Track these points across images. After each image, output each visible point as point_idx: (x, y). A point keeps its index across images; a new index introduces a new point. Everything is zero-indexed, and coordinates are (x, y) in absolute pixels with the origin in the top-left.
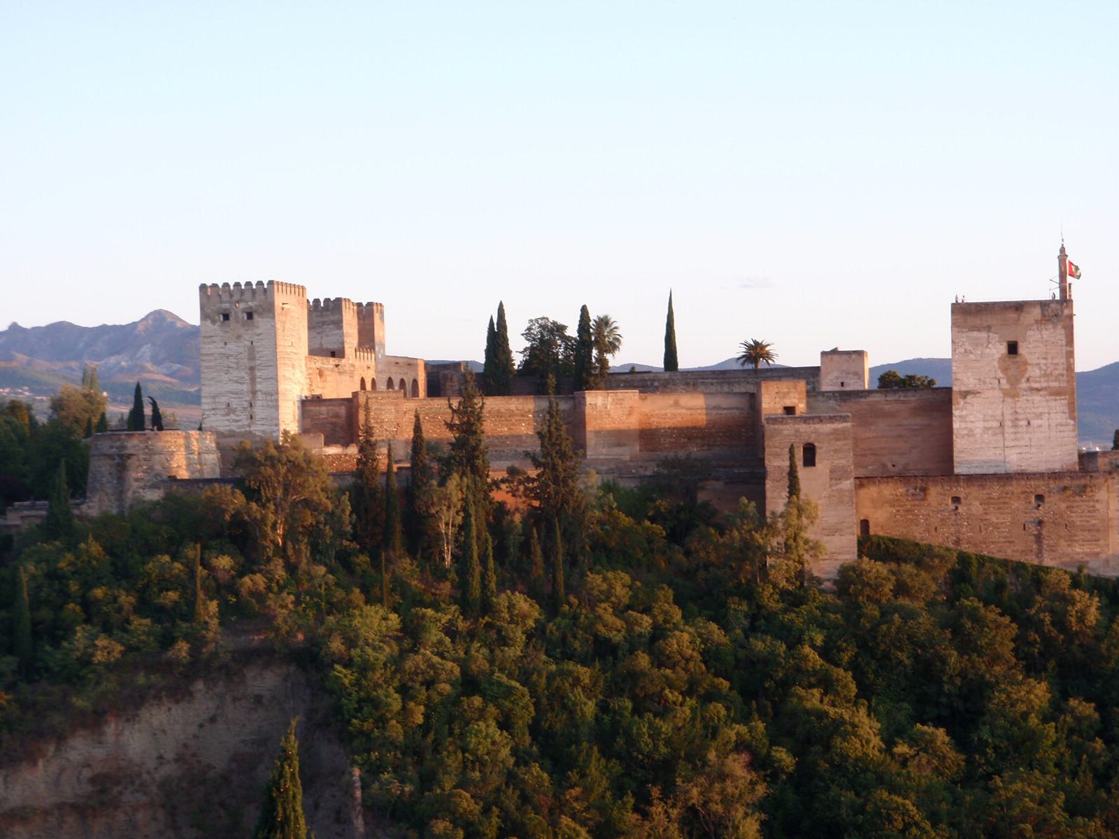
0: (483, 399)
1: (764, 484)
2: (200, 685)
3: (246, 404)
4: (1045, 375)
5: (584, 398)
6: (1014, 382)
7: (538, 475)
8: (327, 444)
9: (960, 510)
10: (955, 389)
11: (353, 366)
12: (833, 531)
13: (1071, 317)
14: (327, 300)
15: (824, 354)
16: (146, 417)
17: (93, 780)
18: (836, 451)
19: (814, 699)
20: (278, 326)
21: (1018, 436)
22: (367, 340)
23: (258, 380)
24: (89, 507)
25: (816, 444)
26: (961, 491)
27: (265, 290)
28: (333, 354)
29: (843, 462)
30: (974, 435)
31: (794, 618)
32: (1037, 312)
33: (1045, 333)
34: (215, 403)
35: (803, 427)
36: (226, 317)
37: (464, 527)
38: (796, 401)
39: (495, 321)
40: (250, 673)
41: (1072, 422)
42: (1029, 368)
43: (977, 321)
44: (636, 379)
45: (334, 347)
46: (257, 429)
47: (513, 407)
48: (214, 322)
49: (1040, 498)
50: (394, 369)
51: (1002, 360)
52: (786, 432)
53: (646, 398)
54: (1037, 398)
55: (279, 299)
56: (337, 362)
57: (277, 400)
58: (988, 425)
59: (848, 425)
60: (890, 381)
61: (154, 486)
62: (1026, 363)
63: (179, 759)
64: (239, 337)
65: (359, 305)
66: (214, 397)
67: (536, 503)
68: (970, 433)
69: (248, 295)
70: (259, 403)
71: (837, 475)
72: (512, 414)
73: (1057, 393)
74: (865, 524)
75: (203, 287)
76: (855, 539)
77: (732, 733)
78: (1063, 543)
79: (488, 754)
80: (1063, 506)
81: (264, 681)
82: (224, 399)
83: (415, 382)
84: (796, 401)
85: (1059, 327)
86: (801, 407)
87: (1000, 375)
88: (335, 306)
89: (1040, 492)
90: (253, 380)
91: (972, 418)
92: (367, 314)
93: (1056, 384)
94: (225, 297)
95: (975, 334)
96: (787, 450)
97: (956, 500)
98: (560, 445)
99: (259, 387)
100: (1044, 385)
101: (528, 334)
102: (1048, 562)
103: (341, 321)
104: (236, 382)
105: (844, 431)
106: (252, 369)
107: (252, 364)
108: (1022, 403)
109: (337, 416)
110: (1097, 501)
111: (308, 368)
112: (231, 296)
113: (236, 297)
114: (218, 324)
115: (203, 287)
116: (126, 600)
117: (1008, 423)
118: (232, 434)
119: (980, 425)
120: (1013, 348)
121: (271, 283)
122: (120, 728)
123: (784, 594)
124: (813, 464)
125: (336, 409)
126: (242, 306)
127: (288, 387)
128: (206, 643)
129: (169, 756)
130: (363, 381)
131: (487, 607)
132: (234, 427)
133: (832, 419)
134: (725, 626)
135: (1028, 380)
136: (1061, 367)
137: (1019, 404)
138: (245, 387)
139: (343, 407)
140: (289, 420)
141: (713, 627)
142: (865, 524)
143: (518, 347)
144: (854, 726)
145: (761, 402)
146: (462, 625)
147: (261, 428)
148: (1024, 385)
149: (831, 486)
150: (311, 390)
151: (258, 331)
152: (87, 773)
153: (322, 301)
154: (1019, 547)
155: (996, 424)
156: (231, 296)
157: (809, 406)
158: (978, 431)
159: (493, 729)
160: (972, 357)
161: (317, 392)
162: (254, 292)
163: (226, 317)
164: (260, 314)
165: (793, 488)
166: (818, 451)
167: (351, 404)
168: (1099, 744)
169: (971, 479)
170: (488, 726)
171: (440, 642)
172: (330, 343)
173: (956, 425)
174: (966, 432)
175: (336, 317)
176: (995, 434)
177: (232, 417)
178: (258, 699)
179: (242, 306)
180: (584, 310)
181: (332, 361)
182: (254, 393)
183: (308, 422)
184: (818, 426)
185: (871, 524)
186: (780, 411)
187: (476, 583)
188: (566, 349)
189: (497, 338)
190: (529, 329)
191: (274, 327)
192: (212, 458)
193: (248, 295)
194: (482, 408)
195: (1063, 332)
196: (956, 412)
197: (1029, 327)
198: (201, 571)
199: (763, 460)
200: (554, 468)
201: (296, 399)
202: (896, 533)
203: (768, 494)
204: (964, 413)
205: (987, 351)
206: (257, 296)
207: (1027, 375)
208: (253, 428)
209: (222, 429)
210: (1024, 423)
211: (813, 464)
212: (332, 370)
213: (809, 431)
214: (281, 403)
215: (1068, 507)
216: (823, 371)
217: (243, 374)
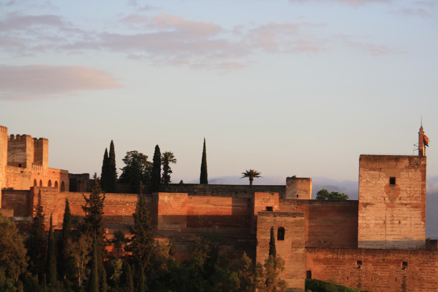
0: (104, 195)
4: (409, 197)
5: (158, 196)
6: (392, 199)
7: (133, 238)
9: (361, 268)
10: (360, 201)
11: (30, 172)
12: (292, 276)
13: (425, 166)
14: (18, 136)
15: (288, 179)
16: (157, 193)
18: (295, 232)
21: (394, 229)
25: (285, 228)
26: (362, 257)
28: (20, 166)
30: (369, 227)
33: (410, 173)
35: (278, 218)
37: (90, 265)
38: (273, 204)
39: (108, 152)
41: (423, 223)
42: (401, 192)
43: (374, 165)
47: (118, 199)
49: (405, 264)
50: (52, 175)
51: (386, 187)
52: (269, 221)
53: (191, 198)
54: (405, 209)
56: (22, 170)
58: (377, 222)
59: (303, 218)
62: (399, 190)
65: (35, 139)
67: (130, 253)
68: (368, 226)
71: (295, 245)
72: (117, 203)
73: (416, 207)
74: (309, 273)
76: (304, 281)
80: (418, 269)
85: (418, 171)
86: (276, 208)
87: (385, 195)
88: (22, 139)
89: (405, 260)
91: (369, 218)
95: (372, 172)
96: (269, 230)
97: (360, 262)
98: (145, 222)
100: (409, 202)
101: (126, 160)
105: (301, 221)
108: (396, 211)
109: (21, 200)
110: (436, 267)
117: (388, 222)
119: (373, 222)
120: (393, 181)
130: (35, 181)
133: (294, 215)
135: (400, 199)
136: (418, 192)
137: (395, 212)
139: (25, 195)
142: (309, 273)
145: (254, 204)
148: (398, 201)
149: (292, 252)
150: (7, 185)
153: (15, 135)
155: (382, 222)
157: (280, 207)
158: (372, 225)
160: (370, 184)
161: (11, 186)
165: (272, 251)
166: (286, 232)
167: (29, 193)
169: (368, 251)
172: (18, 159)
173: (360, 222)
174: (365, 225)
175: (22, 145)
176: (381, 228)
180: (157, 148)
181: (19, 169)
183: (5, 202)
184: (286, 218)
185: (312, 273)
186: (264, 209)
188: (146, 169)
190: (126, 157)
194: (103, 199)
195: (420, 173)
196: (360, 215)
197: (402, 170)
199: (255, 235)
200: (141, 234)
202: (325, 279)
203: (258, 254)
204: (365, 215)
205: (379, 182)
207: (400, 196)
210: (397, 222)
212: (19, 174)
213: (281, 221)
215: (420, 269)
216: (287, 187)
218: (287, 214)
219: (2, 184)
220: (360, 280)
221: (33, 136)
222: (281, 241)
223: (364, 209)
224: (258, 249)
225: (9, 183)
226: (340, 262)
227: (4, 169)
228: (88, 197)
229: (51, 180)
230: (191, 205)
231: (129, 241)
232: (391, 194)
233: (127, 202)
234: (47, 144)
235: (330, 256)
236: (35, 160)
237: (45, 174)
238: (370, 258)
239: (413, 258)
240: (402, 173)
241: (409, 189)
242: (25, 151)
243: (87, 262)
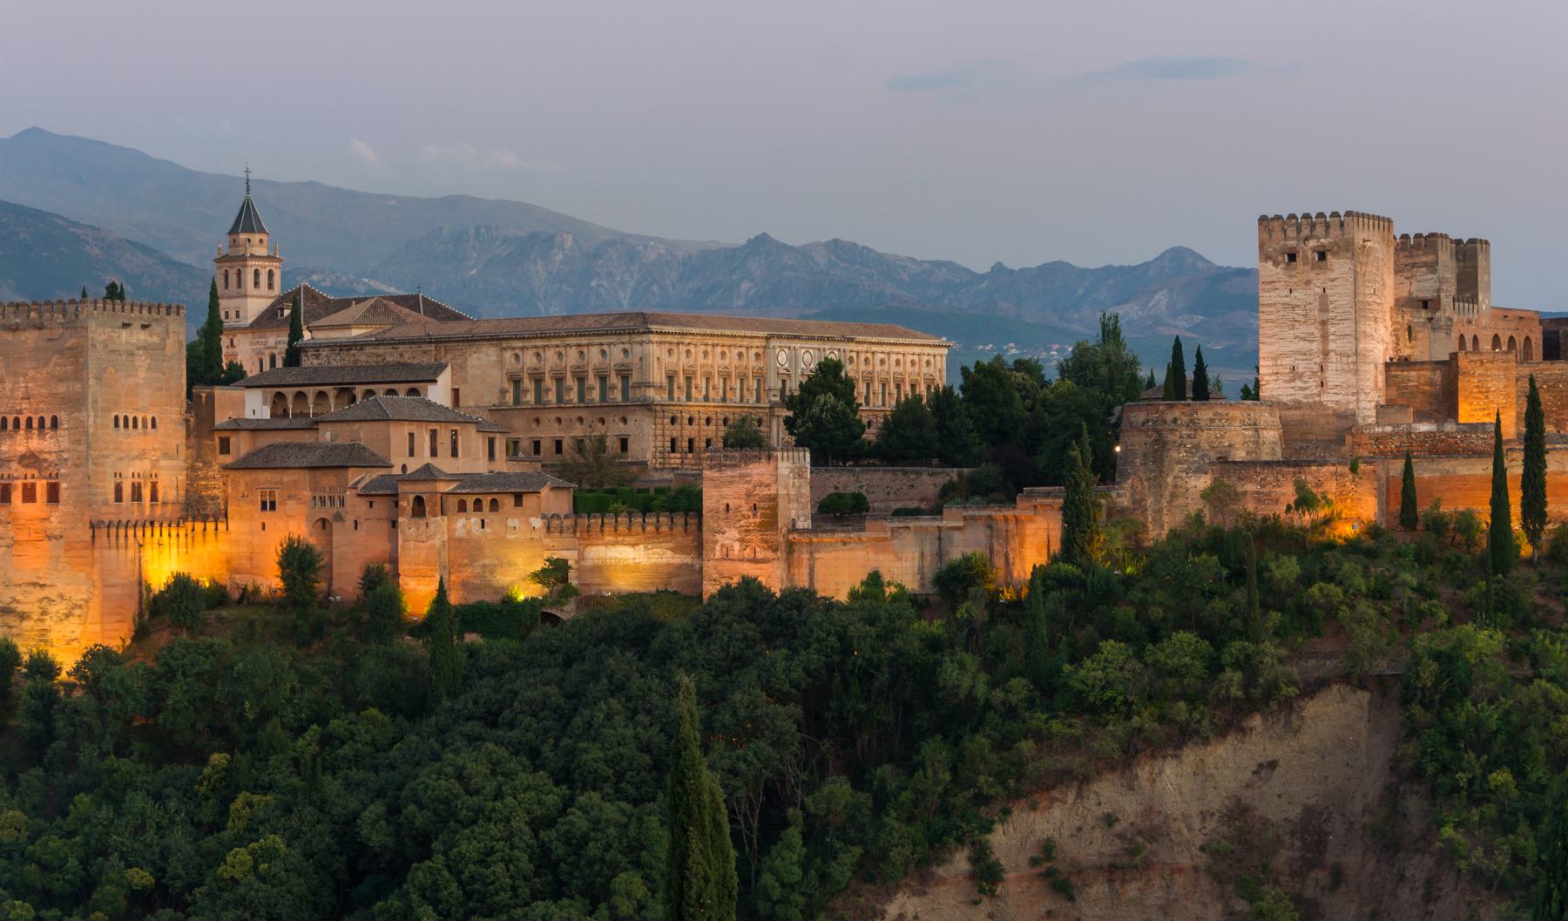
2: (1256, 721)
3: (1316, 368)
8: (1420, 416)
11: (1450, 319)
14: (1418, 236)
22: (1468, 286)
23: (1332, 337)
34: (1276, 365)
36: (1292, 258)
46: (1329, 399)
48: (1276, 264)
50: (1502, 324)
55: (1359, 236)
56: (1430, 315)
61: (1200, 471)
64: (1308, 283)
65: (1459, 242)
66: (1275, 359)
69: (1320, 230)
70: (1332, 366)
75: (1263, 220)
82: (1288, 362)
83: (1527, 339)
88: (1429, 242)
90: (1325, 337)
92: (1469, 255)
94: (1292, 232)
99: (1332, 346)
103: (1437, 263)
104: (1304, 339)
106: (1324, 323)
107: (1324, 316)
111: (1394, 323)
112: (1299, 231)
113: (1306, 232)
114: (1282, 266)
115: (1263, 220)
118: (1298, 405)
121: (1348, 214)
122: (1156, 771)
126: (1312, 243)
127: (1369, 346)
130: (1462, 337)
132: (1299, 396)
138: (1315, 346)
139: (1438, 372)
150: (1397, 350)
151: (1332, 276)
153: (1412, 236)
156: (1299, 231)
161: (1406, 352)
163: (1292, 257)
164: (1335, 254)
175: (1430, 258)
177: (1298, 383)
179: (1312, 243)
181: (1424, 314)
182: (1326, 353)
183: (1393, 393)
192: (1271, 435)
193: (1320, 230)
201: (1381, 361)
206: (1331, 231)
208: (1324, 398)
209: (1285, 399)
212: (1424, 325)
214: (1362, 367)
219: (1387, 349)
221: (1454, 236)
227: (1388, 315)
234: (1487, 252)
236: (1459, 291)
237: (1484, 321)
242: (1434, 271)
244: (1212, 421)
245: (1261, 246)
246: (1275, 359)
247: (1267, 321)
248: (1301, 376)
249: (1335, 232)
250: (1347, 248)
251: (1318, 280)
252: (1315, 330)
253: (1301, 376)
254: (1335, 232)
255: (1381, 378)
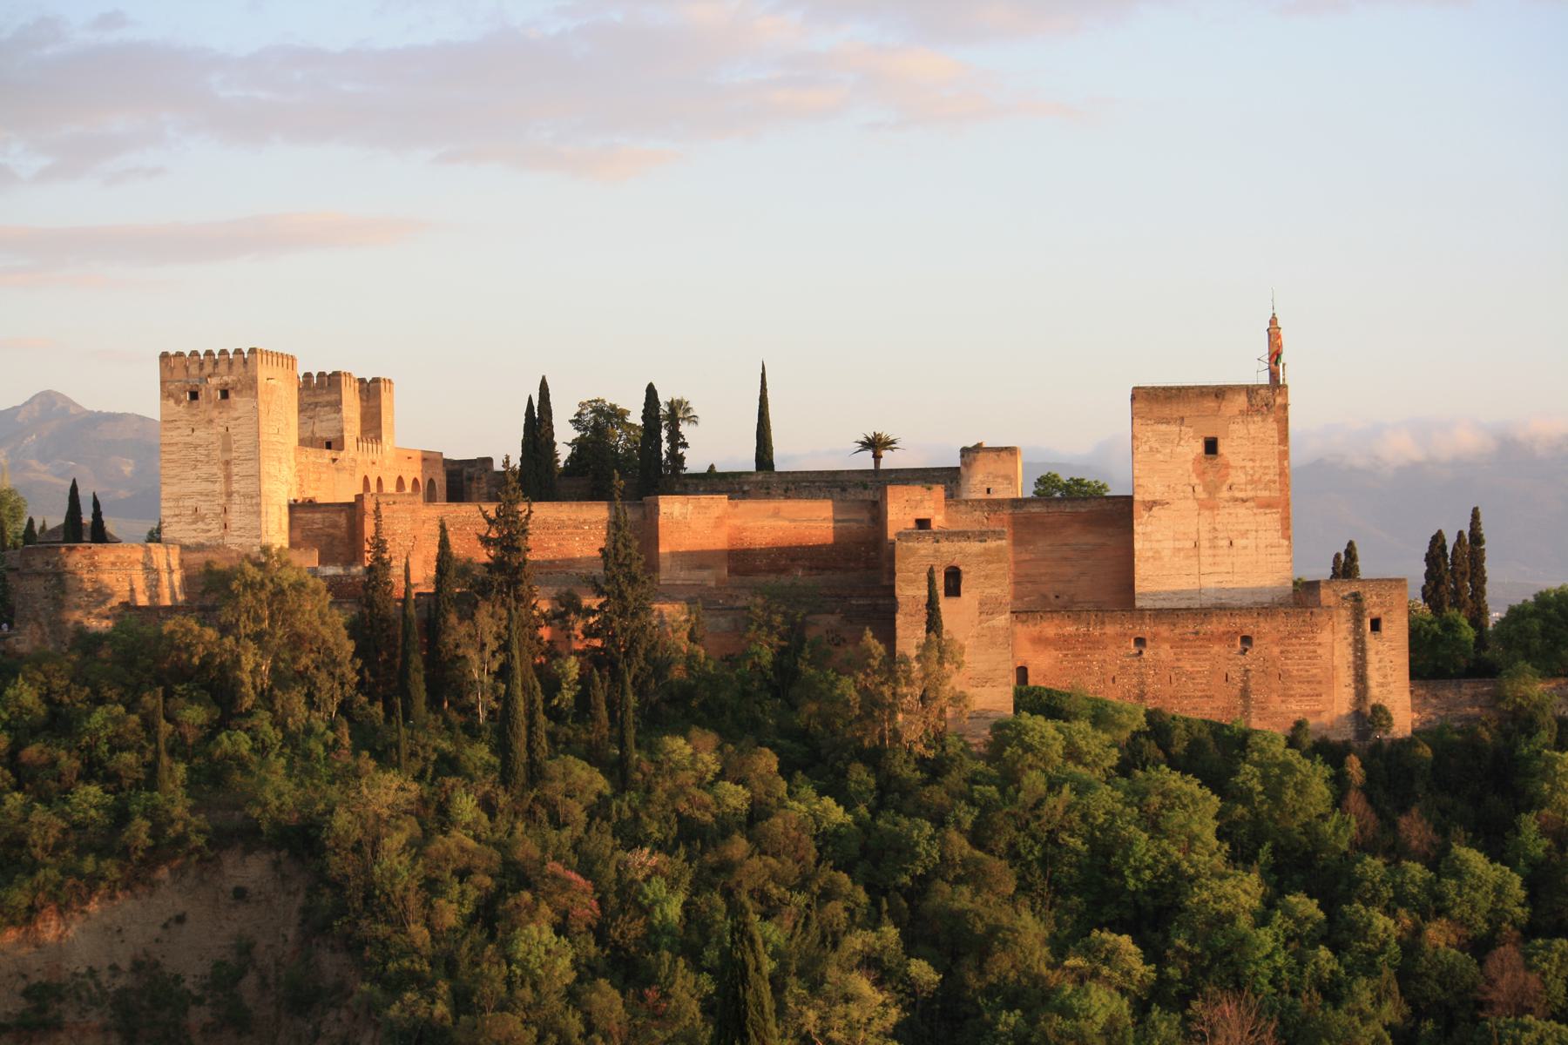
0: (529, 506)
1: (893, 620)
2: (163, 873)
3: (219, 510)
4: (1252, 482)
5: (657, 505)
6: (1212, 490)
7: (601, 606)
9: (1145, 655)
10: (1137, 498)
11: (354, 460)
12: (984, 681)
13: (1285, 407)
14: (321, 375)
16: (654, 497)
17: (26, 993)
18: (986, 577)
19: (963, 898)
20: (262, 408)
21: (1218, 559)
22: (372, 425)
23: (235, 478)
24: (18, 642)
25: (961, 568)
26: (1146, 630)
27: (245, 362)
28: (329, 446)
29: (996, 591)
30: (1161, 558)
31: (936, 795)
32: (1241, 401)
33: (1252, 427)
35: (945, 546)
36: (194, 396)
37: (504, 673)
38: (932, 511)
39: (536, 404)
40: (229, 860)
41: (1285, 543)
42: (1232, 472)
43: (1167, 411)
44: (714, 482)
45: (331, 436)
46: (235, 542)
47: (564, 516)
48: (178, 402)
49: (1247, 640)
51: (1196, 461)
52: (923, 552)
53: (737, 506)
54: (1241, 511)
55: (263, 372)
56: (334, 456)
57: (259, 504)
58: (1178, 545)
59: (1004, 543)
60: (1047, 485)
62: (1227, 466)
63: (137, 966)
64: (211, 421)
65: (362, 381)
66: (177, 500)
67: (598, 643)
68: (1157, 556)
69: (223, 367)
70: (235, 508)
71: (987, 608)
72: (562, 525)
73: (1267, 505)
74: (1022, 673)
76: (1011, 690)
77: (857, 941)
78: (1275, 698)
79: (542, 966)
80: (1276, 650)
81: (252, 870)
82: (189, 503)
84: (932, 511)
86: (938, 521)
87: (1195, 480)
88: (332, 381)
89: (1247, 633)
90: (228, 477)
91: (1159, 537)
92: (371, 391)
93: (1266, 494)
94: (194, 370)
95: (1163, 427)
97: (1140, 642)
98: (629, 566)
99: (235, 487)
100: (1251, 494)
101: (577, 422)
102: (1255, 724)
103: (340, 402)
104: (207, 480)
105: (999, 550)
106: (227, 463)
107: (227, 457)
109: (335, 525)
110: (1320, 644)
111: (298, 464)
113: (208, 369)
114: (184, 404)
116: (69, 763)
117: (1204, 543)
118: (200, 547)
119: (1169, 544)
120: (1211, 447)
121: (253, 351)
123: (922, 761)
124: (958, 594)
125: (334, 517)
126: (214, 381)
128: (172, 821)
129: (125, 965)
130: (366, 478)
131: (536, 774)
132: (202, 538)
133: (982, 536)
134: (847, 802)
136: (1272, 471)
137: (1218, 519)
138: (219, 487)
139: (343, 514)
140: (276, 532)
141: (829, 801)
142: (1022, 673)
143: (564, 436)
144: (1013, 930)
146: (503, 799)
147: (239, 541)
148: (1224, 493)
149: (980, 623)
151: (236, 415)
152: (21, 985)
153: (315, 375)
154: (1221, 704)
157: (948, 520)
158: (1166, 553)
159: (548, 935)
160: (1159, 456)
161: (310, 494)
162: (230, 363)
163: (194, 396)
164: (238, 393)
165: (933, 622)
166: (964, 576)
167: (353, 510)
168: (1324, 953)
169: (1159, 614)
170: (540, 932)
171: (477, 821)
172: (324, 430)
173: (1138, 546)
175: (333, 397)
176: (1188, 557)
177: (201, 525)
178: (240, 894)
179: (214, 381)
180: (651, 391)
181: (328, 454)
182: (229, 495)
183: (298, 534)
184: (964, 544)
185: (1030, 672)
186: (912, 525)
187: (520, 747)
188: (628, 440)
189: (538, 425)
190: (579, 414)
191: (256, 409)
193: (223, 367)
194: (528, 517)
195: (1275, 426)
196: (1138, 528)
197: (1232, 419)
198: (165, 728)
199: (892, 587)
200: (621, 596)
202: (1060, 685)
203: (900, 633)
204: (1149, 529)
205: (1179, 449)
206: (234, 368)
209: (187, 542)
210: (1226, 543)
211: (958, 594)
212: (327, 466)
213: (951, 552)
215: (1282, 652)
216: (963, 470)
217: (215, 470)
218: (965, 535)
220: (1143, 683)
221: (358, 376)
222: (953, 600)
223: (1146, 515)
224: (900, 619)
225: (305, 487)
226: (1095, 644)
227: (292, 454)
228: (492, 514)
229: (35, 520)
230: (738, 522)
231: (593, 613)
232: (1210, 477)
233: (585, 522)
235: (1070, 629)
236: (364, 431)
238: (1164, 630)
239: (1265, 626)
240: (1233, 427)
241: (1251, 464)
242: (339, 411)
243: (495, 666)
244: (113, 564)
245: (163, 383)
246: (177, 500)
247: (169, 461)
248: (203, 518)
249: (238, 369)
250: (251, 385)
251: (221, 418)
252: (218, 470)
253: (203, 518)
254: (238, 369)
255: (285, 520)
